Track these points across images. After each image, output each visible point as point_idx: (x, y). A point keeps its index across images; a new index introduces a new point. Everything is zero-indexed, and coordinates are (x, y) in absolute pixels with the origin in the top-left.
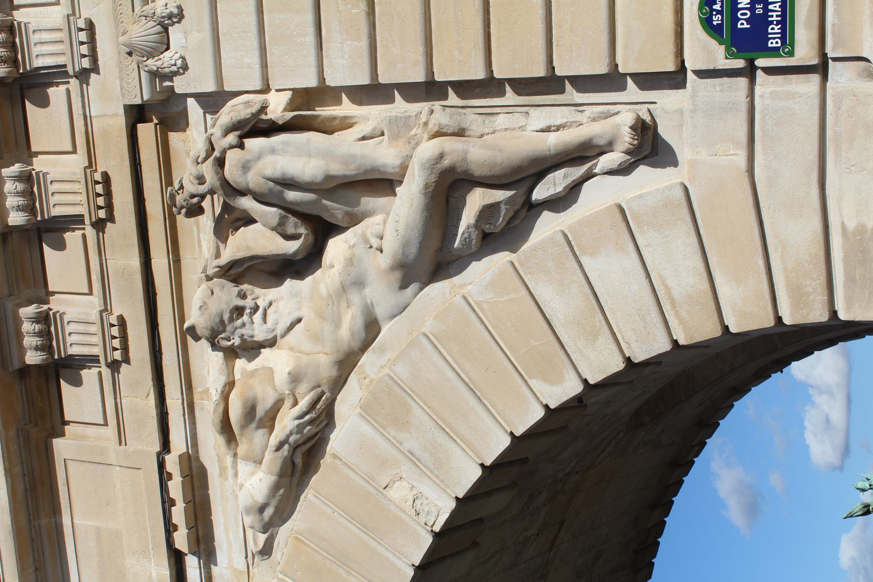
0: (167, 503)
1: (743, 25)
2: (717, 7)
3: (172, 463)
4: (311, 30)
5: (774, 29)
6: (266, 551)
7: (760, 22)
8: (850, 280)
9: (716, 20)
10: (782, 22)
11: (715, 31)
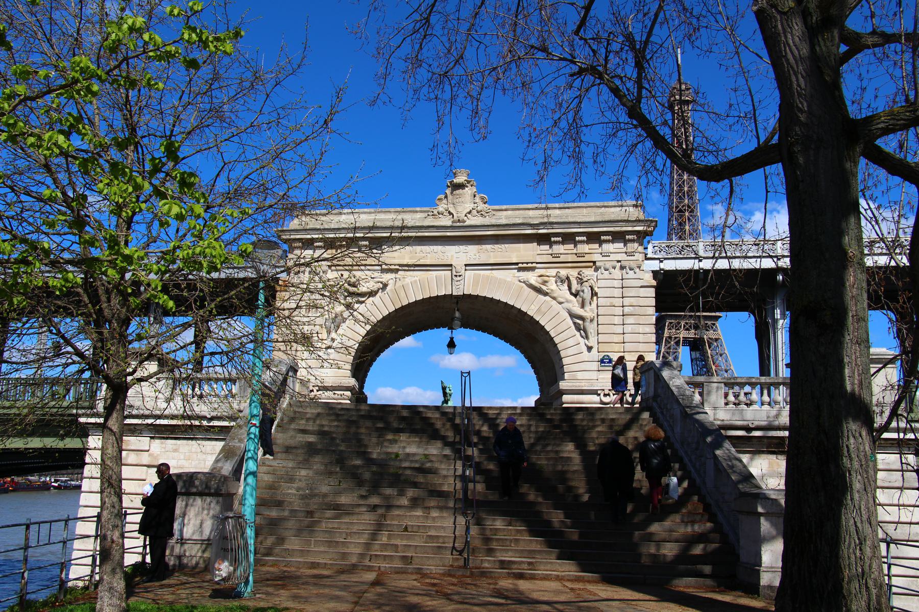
0: (527, 263)
3: (534, 265)
6: (520, 281)
7: (605, 363)
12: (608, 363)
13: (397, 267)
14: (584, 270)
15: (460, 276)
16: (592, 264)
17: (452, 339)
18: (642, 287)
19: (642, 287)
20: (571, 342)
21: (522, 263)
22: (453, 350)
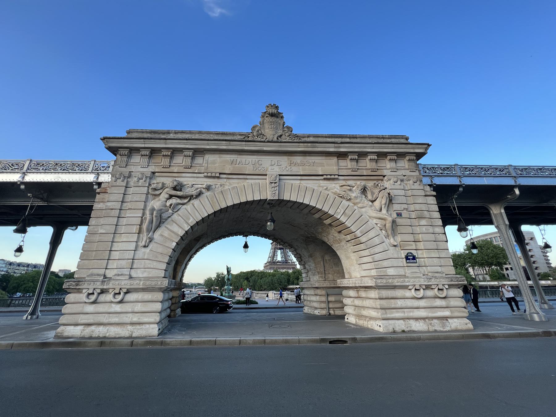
0: (331, 175)
7: (409, 259)
9: (409, 254)
11: (408, 254)
12: (412, 259)
13: (218, 175)
15: (275, 183)
16: (382, 177)
17: (246, 243)
21: (327, 175)
22: (247, 249)
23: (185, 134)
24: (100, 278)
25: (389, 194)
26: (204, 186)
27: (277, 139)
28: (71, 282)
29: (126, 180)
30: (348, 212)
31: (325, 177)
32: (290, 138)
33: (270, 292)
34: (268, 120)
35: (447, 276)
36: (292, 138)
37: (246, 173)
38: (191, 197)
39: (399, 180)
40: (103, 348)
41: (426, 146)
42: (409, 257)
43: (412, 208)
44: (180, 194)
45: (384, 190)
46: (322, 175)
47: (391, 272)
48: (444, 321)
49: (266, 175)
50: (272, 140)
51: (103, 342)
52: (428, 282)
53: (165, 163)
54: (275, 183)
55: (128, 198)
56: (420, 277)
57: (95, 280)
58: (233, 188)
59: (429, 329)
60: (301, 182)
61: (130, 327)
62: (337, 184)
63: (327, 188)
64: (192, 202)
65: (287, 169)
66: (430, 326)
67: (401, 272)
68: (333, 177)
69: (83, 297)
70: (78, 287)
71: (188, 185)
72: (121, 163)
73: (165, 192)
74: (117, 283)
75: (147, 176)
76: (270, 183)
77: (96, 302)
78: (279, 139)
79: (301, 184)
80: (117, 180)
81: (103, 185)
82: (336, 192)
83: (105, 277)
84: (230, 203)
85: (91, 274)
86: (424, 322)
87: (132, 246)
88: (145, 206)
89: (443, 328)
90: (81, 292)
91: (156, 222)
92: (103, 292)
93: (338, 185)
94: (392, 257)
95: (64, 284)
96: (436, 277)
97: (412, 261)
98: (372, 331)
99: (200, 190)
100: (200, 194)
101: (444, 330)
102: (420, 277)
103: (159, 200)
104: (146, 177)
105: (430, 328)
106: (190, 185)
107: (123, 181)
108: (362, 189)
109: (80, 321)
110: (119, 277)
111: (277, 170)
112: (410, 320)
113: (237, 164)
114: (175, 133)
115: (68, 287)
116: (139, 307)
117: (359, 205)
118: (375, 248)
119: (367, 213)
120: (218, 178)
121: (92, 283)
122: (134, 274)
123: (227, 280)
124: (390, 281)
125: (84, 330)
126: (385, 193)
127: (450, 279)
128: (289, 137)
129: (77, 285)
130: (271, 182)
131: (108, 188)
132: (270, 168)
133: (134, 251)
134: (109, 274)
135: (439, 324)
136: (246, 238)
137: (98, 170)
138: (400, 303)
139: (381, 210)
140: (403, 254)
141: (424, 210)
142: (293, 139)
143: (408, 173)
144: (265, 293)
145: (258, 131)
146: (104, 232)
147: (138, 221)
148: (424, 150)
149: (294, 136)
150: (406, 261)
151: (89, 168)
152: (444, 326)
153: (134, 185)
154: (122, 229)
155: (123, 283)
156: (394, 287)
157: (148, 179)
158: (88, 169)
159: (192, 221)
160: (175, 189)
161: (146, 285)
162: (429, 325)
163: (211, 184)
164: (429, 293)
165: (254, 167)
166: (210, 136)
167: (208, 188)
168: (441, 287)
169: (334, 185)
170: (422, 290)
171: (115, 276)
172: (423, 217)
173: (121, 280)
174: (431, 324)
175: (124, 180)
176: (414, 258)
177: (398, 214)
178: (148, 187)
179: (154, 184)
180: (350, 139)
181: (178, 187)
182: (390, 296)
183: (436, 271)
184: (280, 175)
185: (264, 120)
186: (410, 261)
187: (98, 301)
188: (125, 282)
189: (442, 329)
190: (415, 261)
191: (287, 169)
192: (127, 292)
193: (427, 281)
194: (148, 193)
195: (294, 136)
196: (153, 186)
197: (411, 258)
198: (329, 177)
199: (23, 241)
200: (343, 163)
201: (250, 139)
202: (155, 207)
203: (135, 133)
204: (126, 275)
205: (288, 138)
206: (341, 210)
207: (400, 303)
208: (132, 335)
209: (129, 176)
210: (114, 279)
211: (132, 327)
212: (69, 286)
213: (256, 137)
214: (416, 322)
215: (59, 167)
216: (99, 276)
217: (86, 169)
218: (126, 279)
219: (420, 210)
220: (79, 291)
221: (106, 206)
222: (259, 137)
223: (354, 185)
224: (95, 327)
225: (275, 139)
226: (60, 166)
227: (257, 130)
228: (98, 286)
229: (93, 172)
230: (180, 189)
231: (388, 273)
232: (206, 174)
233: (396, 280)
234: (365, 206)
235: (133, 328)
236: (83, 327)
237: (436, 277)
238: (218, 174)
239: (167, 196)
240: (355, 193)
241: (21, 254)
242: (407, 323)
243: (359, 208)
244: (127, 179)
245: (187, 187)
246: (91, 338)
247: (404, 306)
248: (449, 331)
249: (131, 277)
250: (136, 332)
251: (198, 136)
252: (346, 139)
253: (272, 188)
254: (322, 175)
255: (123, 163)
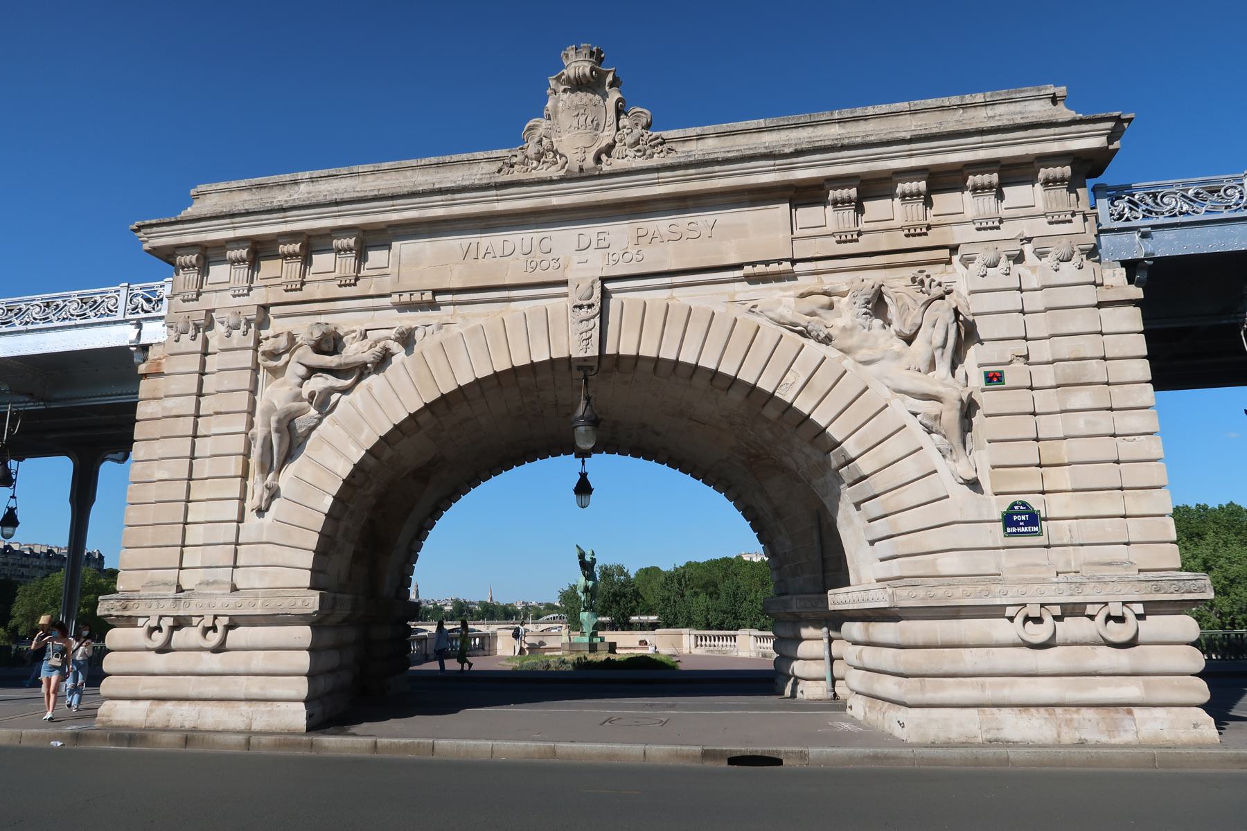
0: (767, 263)
1: (1015, 518)
2: (1021, 508)
4: (1001, 336)
5: (1014, 530)
7: (1016, 524)
8: (916, 562)
9: (1016, 508)
10: (1017, 532)
11: (1012, 507)
12: (1027, 524)
13: (428, 296)
14: (929, 269)
15: (590, 306)
16: (945, 254)
17: (583, 476)
18: (1100, 305)
19: (1100, 305)
20: (909, 468)
21: (754, 264)
22: (587, 497)
23: (338, 180)
24: (169, 591)
25: (957, 312)
26: (392, 333)
27: (598, 159)
28: (112, 602)
29: (200, 336)
30: (822, 381)
31: (748, 270)
32: (639, 151)
33: (739, 632)
34: (568, 103)
35: (1142, 576)
36: (645, 151)
37: (507, 282)
38: (360, 371)
39: (1004, 258)
40: (190, 749)
41: (1110, 125)
42: (1015, 518)
43: (1041, 351)
44: (331, 362)
45: (942, 298)
46: (739, 266)
47: (948, 564)
48: (1119, 716)
49: (565, 283)
50: (581, 169)
51: (189, 736)
52: (1071, 595)
53: (289, 276)
54: (590, 306)
55: (210, 384)
56: (1043, 581)
57: (159, 595)
58: (474, 331)
59: (1059, 736)
60: (674, 295)
61: (244, 707)
62: (789, 288)
63: (754, 307)
64: (364, 382)
65: (628, 257)
66: (1064, 729)
67: (987, 563)
68: (773, 267)
69: (135, 635)
70: (127, 613)
71: (354, 335)
72: (186, 288)
73: (296, 360)
74: (206, 602)
75: (248, 317)
76: (575, 307)
77: (167, 648)
78: (604, 157)
79: (674, 302)
80: (179, 336)
81: (152, 354)
82: (782, 317)
83: (180, 589)
84: (465, 379)
85: (151, 582)
86: (1047, 716)
87: (232, 510)
88: (253, 404)
89: (1108, 735)
90: (135, 626)
91: (280, 445)
92: (180, 623)
93: (792, 293)
94: (960, 519)
95: (99, 606)
96: (1100, 581)
97: (1026, 529)
98: (888, 739)
99: (384, 346)
100: (383, 360)
101: (1113, 741)
102: (1043, 581)
103: (283, 384)
104: (248, 322)
105: (1062, 734)
106: (358, 333)
107: (194, 338)
108: (868, 303)
109: (141, 692)
110: (209, 588)
111: (598, 265)
112: (1000, 711)
113: (481, 257)
114: (313, 182)
115: (106, 613)
116: (259, 661)
117: (864, 354)
118: (899, 493)
119: (887, 378)
120: (433, 306)
121: (154, 603)
122: (241, 579)
123: (583, 593)
124: (940, 592)
125: (151, 711)
126: (942, 312)
127: (1153, 583)
128: (636, 149)
129: (125, 608)
130: (579, 303)
131: (164, 360)
132: (577, 257)
133: (236, 523)
134: (189, 580)
135: (1098, 724)
136: (583, 462)
137: (138, 312)
138: (969, 659)
139: (932, 365)
140: (998, 507)
141: (1089, 355)
142: (648, 152)
143: (1040, 227)
144: (726, 636)
145: (540, 141)
146: (166, 476)
147: (238, 444)
148: (1104, 138)
149: (652, 143)
150: (1005, 530)
151: (117, 308)
152: (1113, 729)
153: (220, 348)
154: (203, 468)
155: (219, 603)
156: (955, 613)
157: (253, 325)
158: (116, 312)
159: (369, 438)
160: (318, 348)
161: (269, 607)
162: (1062, 725)
163: (413, 326)
164: (1073, 627)
165: (529, 260)
166: (406, 177)
167: (407, 339)
168: (1116, 610)
169: (782, 293)
170: (1048, 619)
171: (201, 586)
172: (1082, 381)
173: (214, 596)
174: (1069, 722)
175: (196, 336)
176: (1034, 519)
177: (991, 375)
178: (256, 350)
179: (267, 339)
180: (843, 127)
181: (330, 343)
182: (939, 638)
183: (1108, 560)
184: (604, 280)
185: (558, 102)
186: (1019, 529)
187: (173, 644)
188: (224, 600)
189: (1104, 739)
190: (1036, 529)
191: (628, 257)
192: (230, 627)
193: (1068, 593)
194: (255, 369)
195: (652, 143)
196: (266, 346)
197: (1022, 521)
198: (760, 269)
199: (13, 497)
200: (809, 216)
201: (516, 175)
202: (276, 404)
203: (213, 195)
204: (223, 583)
205: (631, 153)
206: (797, 377)
207: (969, 659)
208: (251, 726)
209: (210, 326)
210: (199, 594)
211: (250, 707)
212: (108, 610)
213: (535, 164)
214: (1018, 716)
215: (54, 312)
216: (166, 587)
217: (111, 311)
218: (224, 594)
219: (1073, 356)
220: (130, 621)
221: (164, 408)
222: (544, 162)
223: (845, 288)
224: (174, 706)
225: (589, 162)
226: (55, 309)
227: (537, 139)
228: (166, 609)
229: (128, 317)
230: (331, 349)
231: (939, 568)
232: (395, 298)
233: (961, 589)
234: (879, 356)
235: (252, 709)
236: (148, 703)
237: (1100, 581)
238: (430, 293)
239: (302, 371)
240: (847, 314)
241: (14, 532)
242: (990, 716)
243: (861, 362)
244: (204, 332)
245: (350, 340)
246: (166, 729)
247: (983, 666)
248: (1127, 746)
249: (234, 589)
250: (258, 718)
251: (374, 181)
252: (831, 126)
253: (581, 321)
254: (739, 266)
255: (190, 287)
